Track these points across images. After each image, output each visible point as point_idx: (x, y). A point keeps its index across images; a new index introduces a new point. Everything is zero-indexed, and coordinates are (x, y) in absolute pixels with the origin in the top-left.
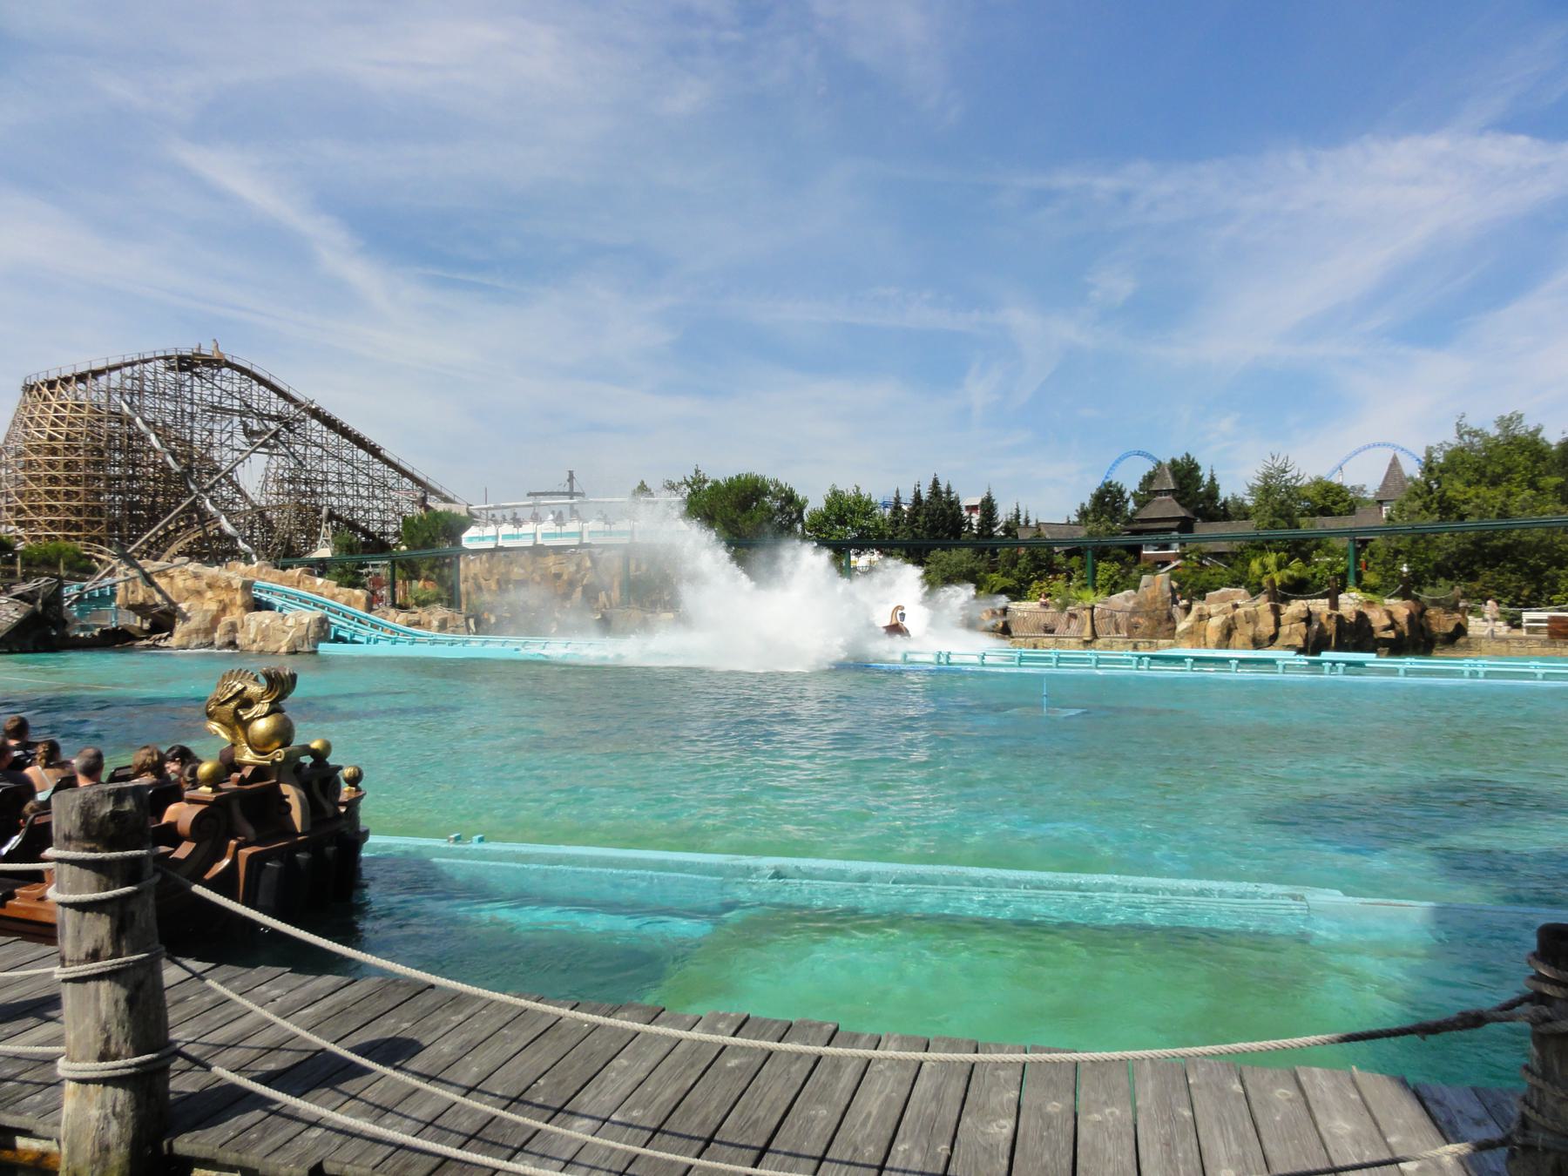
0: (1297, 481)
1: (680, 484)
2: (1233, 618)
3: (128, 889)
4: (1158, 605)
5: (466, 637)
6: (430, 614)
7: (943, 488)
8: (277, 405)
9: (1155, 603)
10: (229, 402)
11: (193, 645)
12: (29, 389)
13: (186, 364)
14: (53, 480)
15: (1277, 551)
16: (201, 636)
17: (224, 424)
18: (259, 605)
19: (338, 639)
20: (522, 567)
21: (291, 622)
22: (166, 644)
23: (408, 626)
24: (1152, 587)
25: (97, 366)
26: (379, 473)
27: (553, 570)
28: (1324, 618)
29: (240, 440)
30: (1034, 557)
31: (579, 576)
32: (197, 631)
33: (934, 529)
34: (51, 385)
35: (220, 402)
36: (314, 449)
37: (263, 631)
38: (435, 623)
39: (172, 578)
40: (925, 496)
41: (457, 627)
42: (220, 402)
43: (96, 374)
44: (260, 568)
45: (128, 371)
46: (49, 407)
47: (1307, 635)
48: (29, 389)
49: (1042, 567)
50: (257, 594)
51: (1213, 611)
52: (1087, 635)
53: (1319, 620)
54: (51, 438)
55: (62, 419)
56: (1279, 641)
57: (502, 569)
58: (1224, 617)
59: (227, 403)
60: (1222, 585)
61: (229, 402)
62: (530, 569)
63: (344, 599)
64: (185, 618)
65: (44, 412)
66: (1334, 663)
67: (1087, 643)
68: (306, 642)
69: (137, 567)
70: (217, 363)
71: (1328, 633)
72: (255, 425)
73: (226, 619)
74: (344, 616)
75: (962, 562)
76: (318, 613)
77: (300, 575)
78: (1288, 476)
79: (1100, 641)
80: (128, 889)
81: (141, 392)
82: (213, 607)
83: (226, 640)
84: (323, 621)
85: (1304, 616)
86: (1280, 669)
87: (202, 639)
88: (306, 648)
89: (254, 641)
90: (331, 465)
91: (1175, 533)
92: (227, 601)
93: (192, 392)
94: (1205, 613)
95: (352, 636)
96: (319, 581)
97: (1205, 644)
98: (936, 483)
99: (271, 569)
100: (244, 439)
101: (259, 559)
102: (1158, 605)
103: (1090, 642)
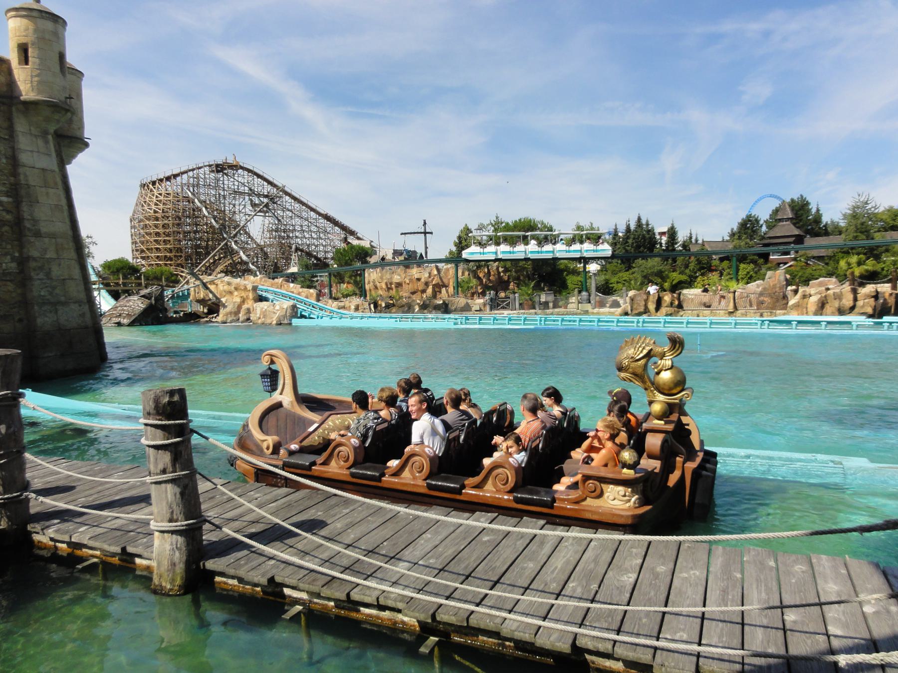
0: (876, 209)
1: (488, 225)
2: (826, 296)
3: (178, 439)
4: (777, 289)
5: (369, 314)
6: (350, 302)
7: (644, 222)
8: (267, 189)
9: (775, 288)
10: (243, 188)
11: (228, 321)
12: (143, 186)
13: (220, 168)
14: (157, 234)
15: (858, 254)
16: (233, 315)
17: (241, 200)
18: (261, 299)
19: (303, 316)
20: (399, 275)
21: (277, 307)
22: (215, 320)
24: (774, 279)
25: (176, 172)
27: (416, 276)
28: (887, 296)
30: (699, 262)
32: (231, 313)
33: (638, 247)
34: (154, 183)
35: (238, 189)
36: (288, 212)
37: (264, 312)
38: (353, 307)
39: (217, 285)
40: (633, 227)
42: (238, 189)
43: (175, 176)
44: (261, 279)
45: (191, 174)
46: (153, 195)
47: (875, 306)
48: (143, 186)
49: (705, 268)
50: (260, 293)
51: (812, 292)
52: (731, 308)
53: (884, 297)
54: (155, 212)
55: (160, 201)
56: (856, 310)
57: (388, 276)
58: (820, 296)
59: (242, 189)
60: (820, 276)
61: (243, 188)
62: (403, 276)
64: (225, 306)
65: (151, 198)
66: (891, 323)
67: (731, 313)
69: (199, 279)
70: (235, 167)
71: (889, 305)
73: (245, 307)
74: (305, 304)
75: (654, 266)
76: (291, 302)
78: (869, 207)
79: (739, 312)
80: (178, 439)
81: (198, 185)
82: (238, 300)
84: (294, 307)
85: (874, 294)
86: (854, 327)
87: (233, 317)
88: (286, 322)
89: (259, 318)
90: (297, 221)
91: (792, 245)
92: (245, 297)
93: (223, 183)
94: (807, 294)
95: (309, 315)
96: (292, 285)
97: (807, 313)
98: (639, 219)
99: (267, 279)
100: (251, 208)
101: (260, 274)
102: (777, 289)
103: (732, 312)
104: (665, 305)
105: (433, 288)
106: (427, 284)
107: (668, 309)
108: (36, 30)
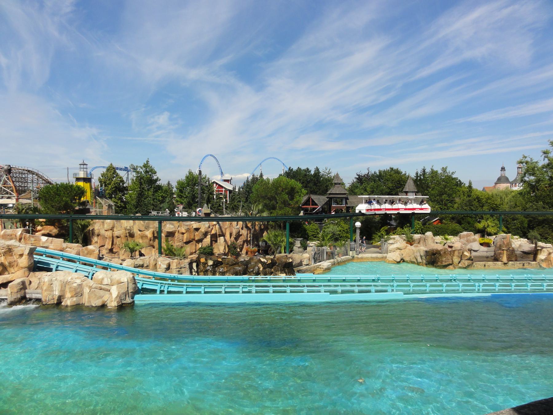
23: (135, 267)
24: (506, 240)
31: (210, 229)
41: (181, 268)
63: (75, 251)
68: (127, 296)
74: (63, 259)
77: (21, 234)
83: (19, 296)
103: (506, 263)
104: (466, 258)
105: (211, 237)
106: (205, 234)
107: (469, 261)
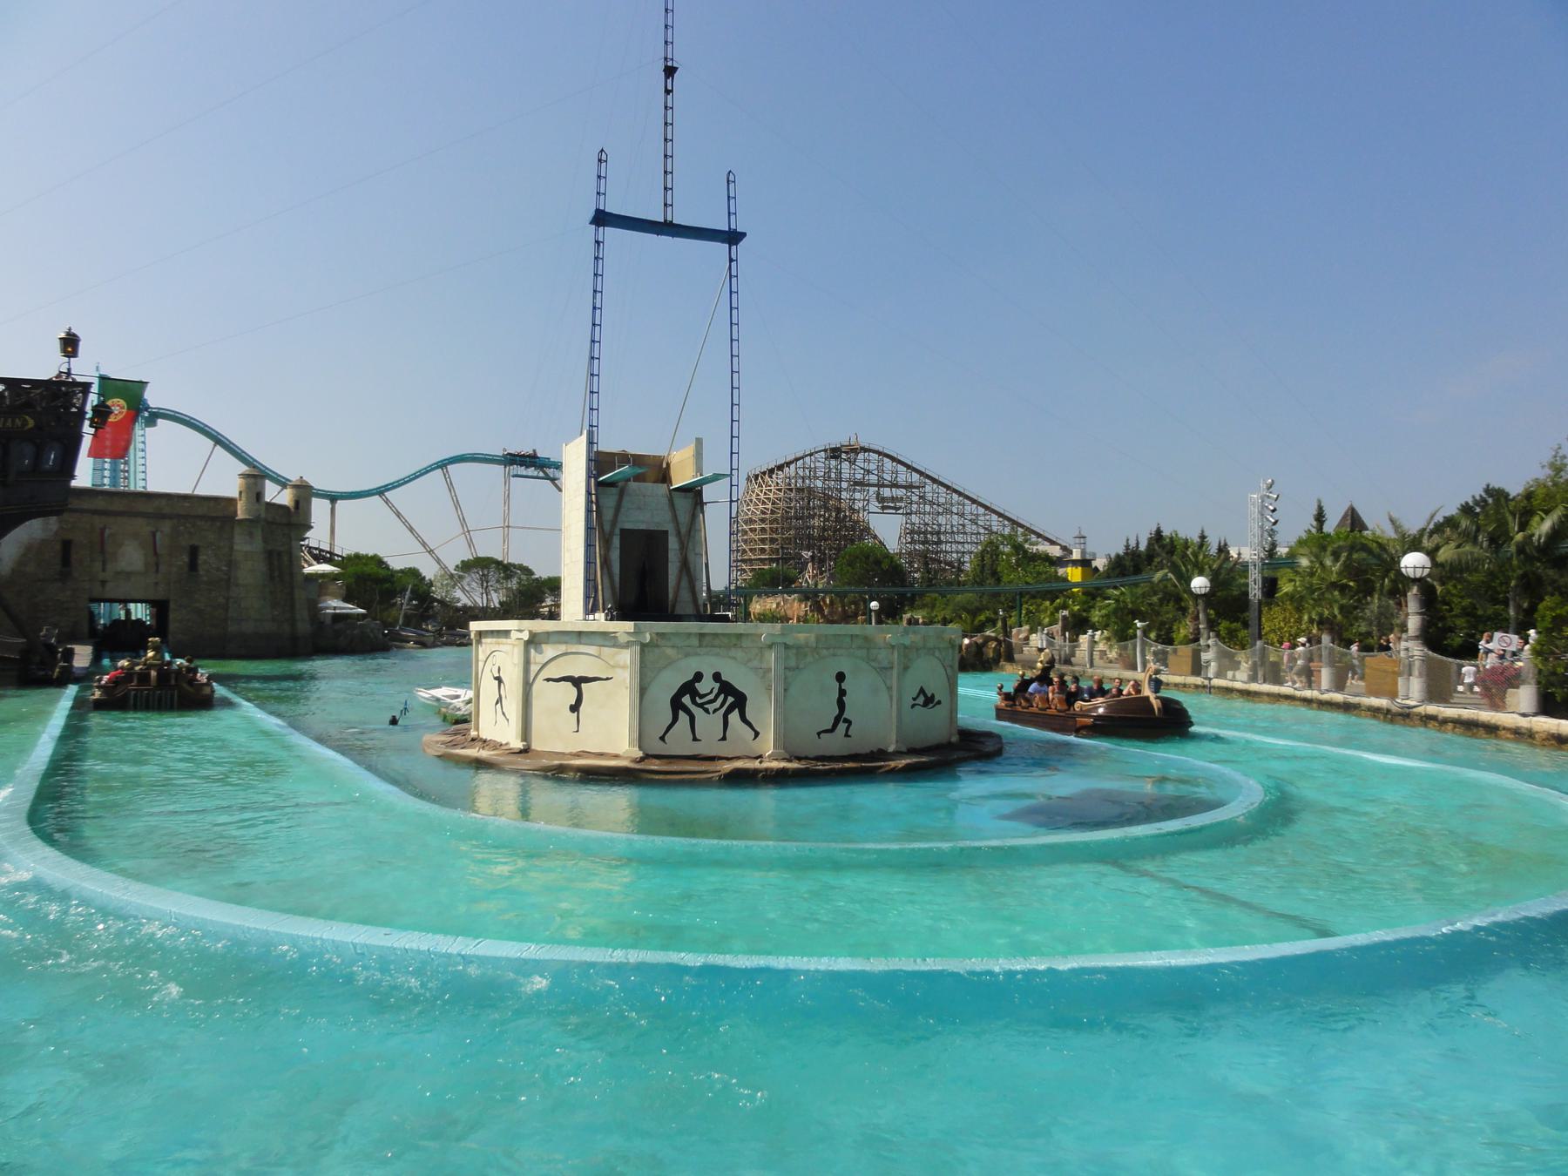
8: (904, 476)
13: (835, 453)
26: (988, 523)
29: (874, 506)
45: (800, 463)
46: (761, 491)
65: (759, 495)
70: (855, 451)
72: (887, 492)
100: (877, 504)
108: (246, 484)
